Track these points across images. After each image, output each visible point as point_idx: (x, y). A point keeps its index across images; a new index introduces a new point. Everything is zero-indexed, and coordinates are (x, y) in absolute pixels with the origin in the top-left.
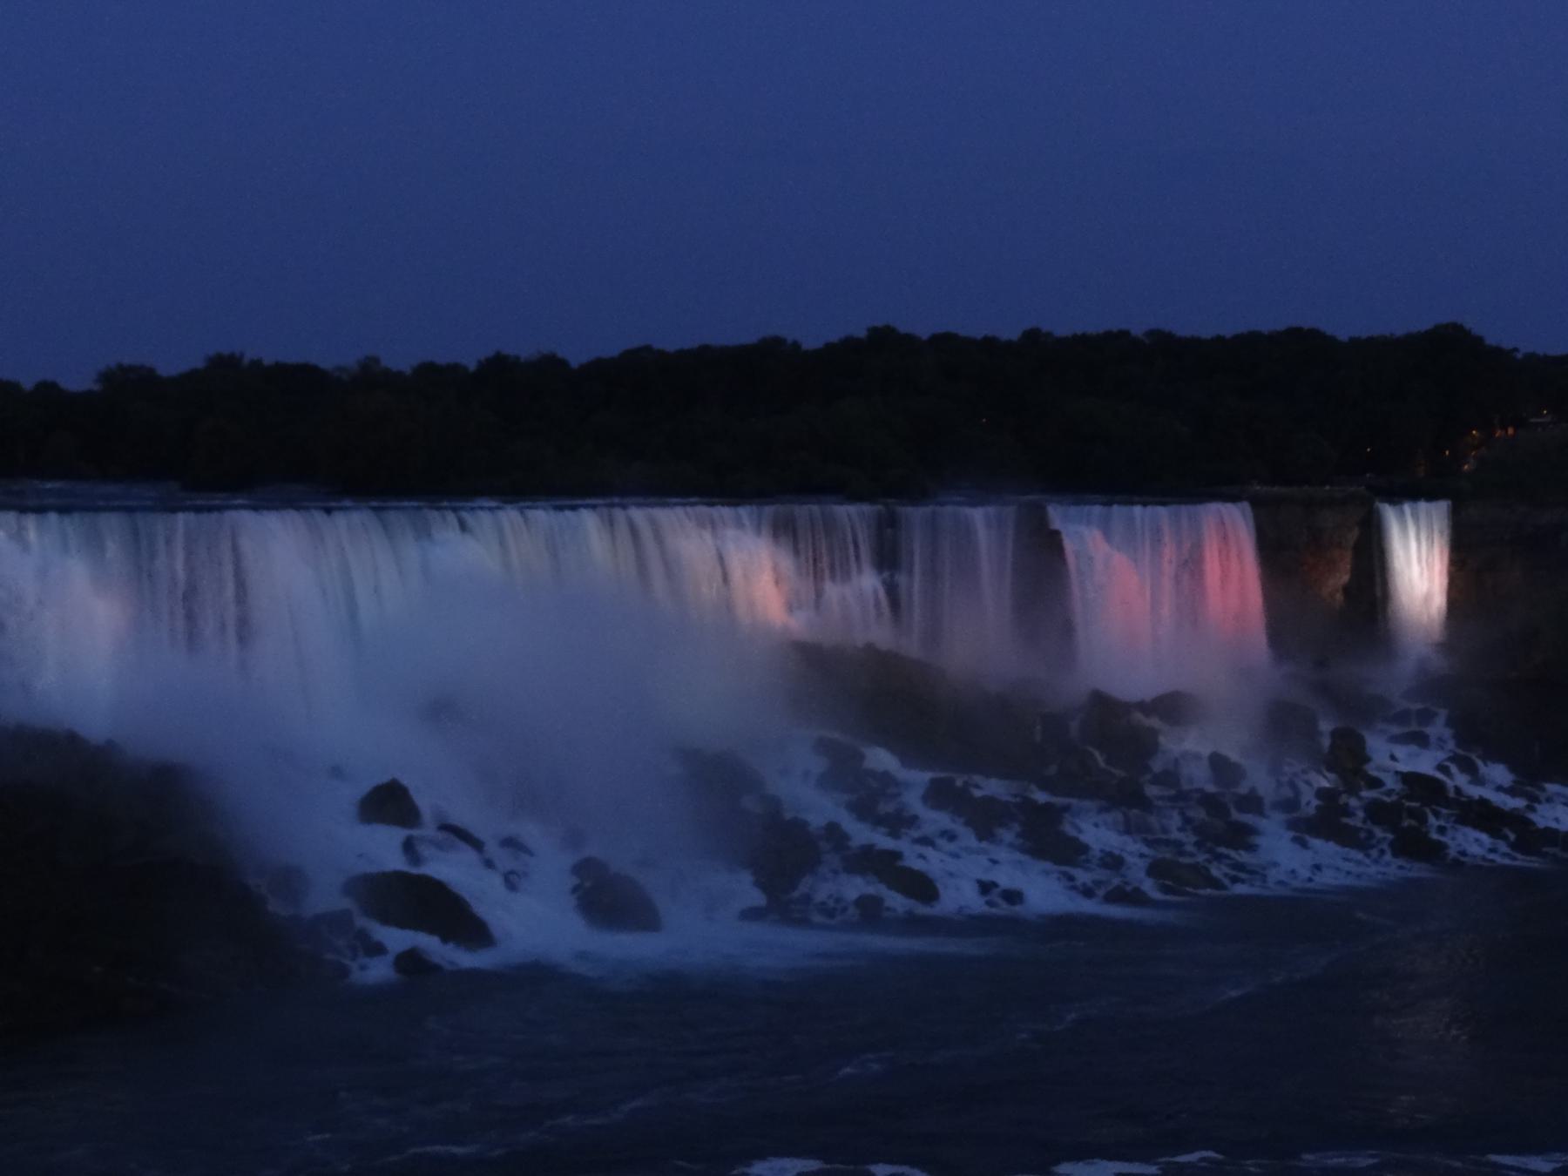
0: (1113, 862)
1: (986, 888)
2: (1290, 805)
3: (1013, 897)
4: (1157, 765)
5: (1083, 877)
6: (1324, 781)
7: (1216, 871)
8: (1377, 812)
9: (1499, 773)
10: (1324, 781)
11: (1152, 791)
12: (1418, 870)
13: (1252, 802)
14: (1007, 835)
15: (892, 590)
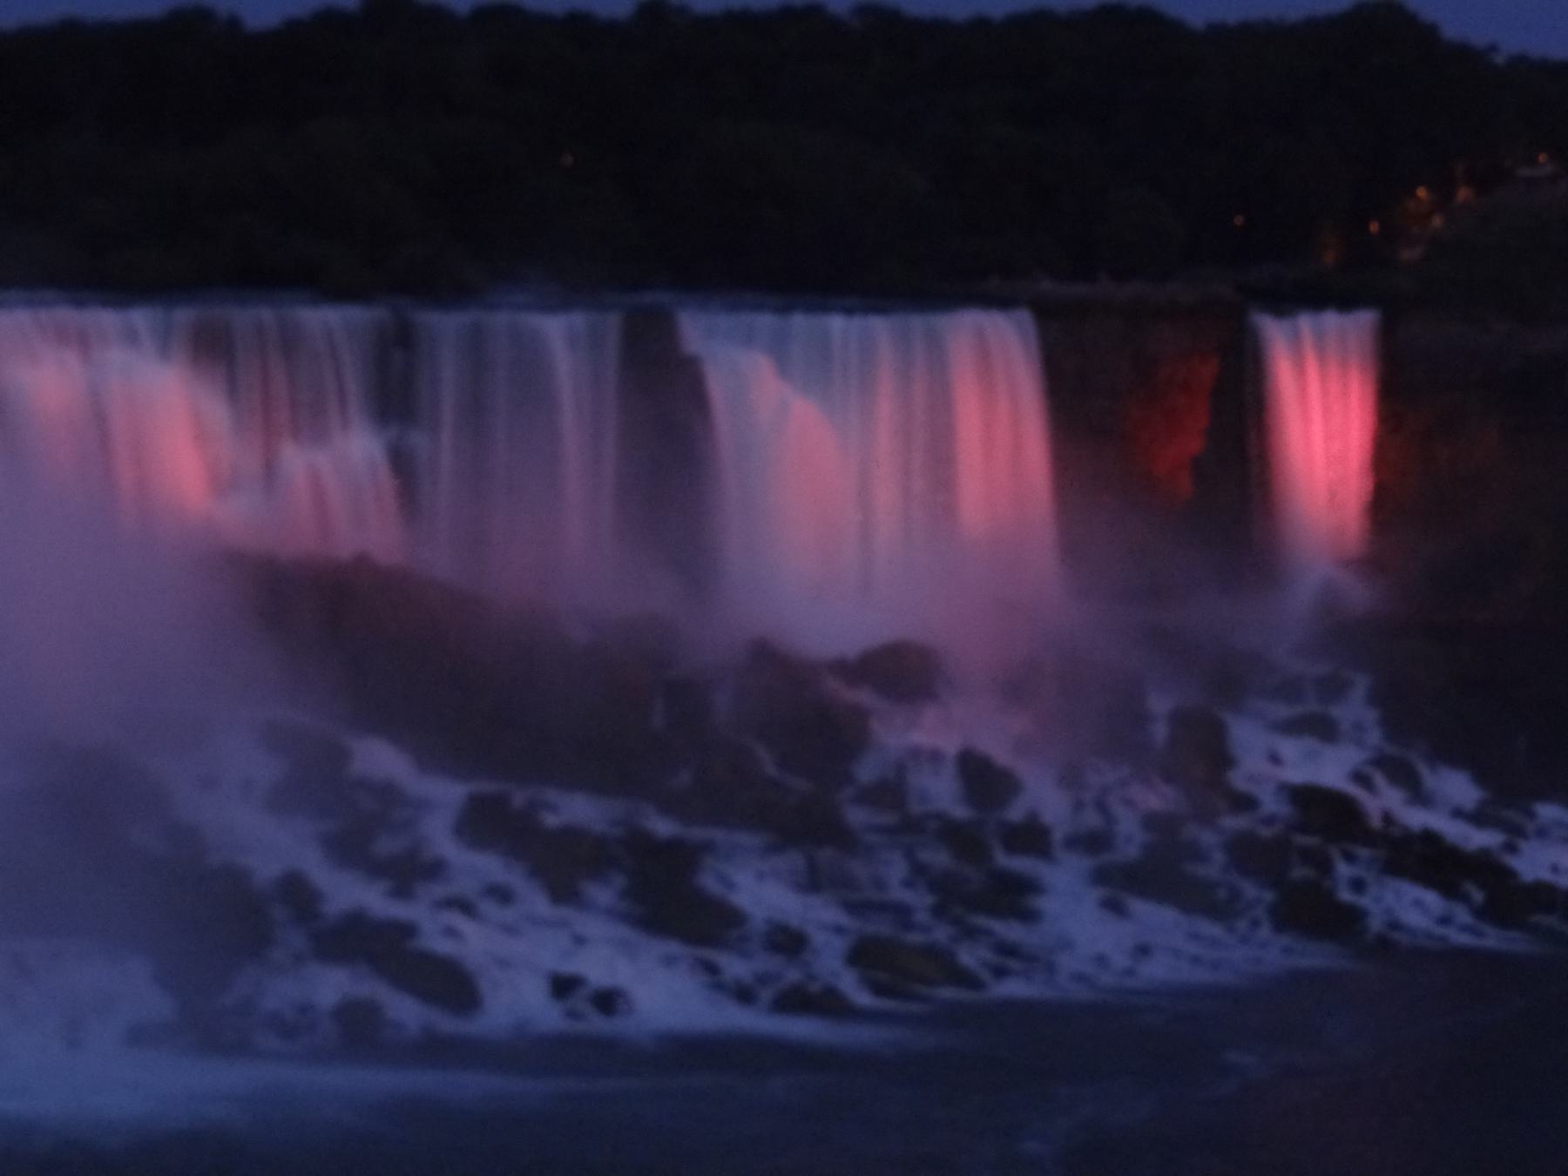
0: (788, 941)
1: (563, 986)
2: (1093, 842)
3: (608, 1001)
4: (867, 771)
5: (735, 967)
6: (1157, 798)
7: (970, 957)
8: (1245, 852)
9: (1458, 787)
10: (1157, 798)
11: (857, 816)
12: (1316, 956)
13: (1032, 838)
14: (602, 894)
15: (401, 463)
